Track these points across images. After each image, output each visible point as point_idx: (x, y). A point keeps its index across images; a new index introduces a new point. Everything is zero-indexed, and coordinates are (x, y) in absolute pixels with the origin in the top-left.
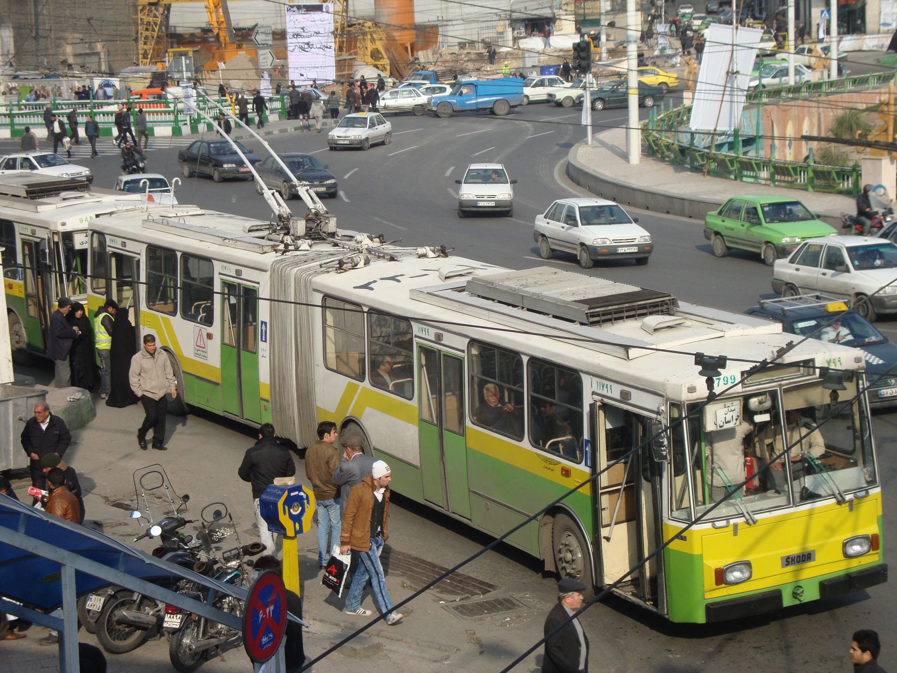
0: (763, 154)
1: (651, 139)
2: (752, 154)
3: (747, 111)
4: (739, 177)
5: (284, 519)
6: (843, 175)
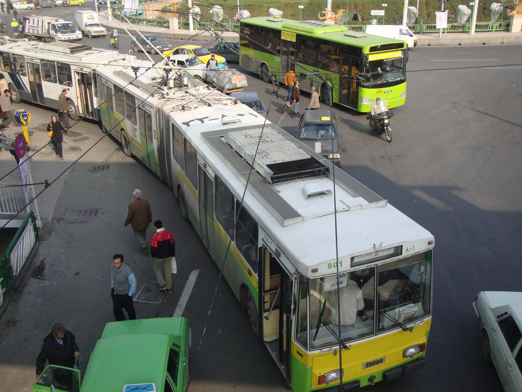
0: (144, 17)
1: (114, 13)
2: (141, 17)
3: (139, 6)
4: (138, 23)
5: (22, 121)
6: (165, 23)
